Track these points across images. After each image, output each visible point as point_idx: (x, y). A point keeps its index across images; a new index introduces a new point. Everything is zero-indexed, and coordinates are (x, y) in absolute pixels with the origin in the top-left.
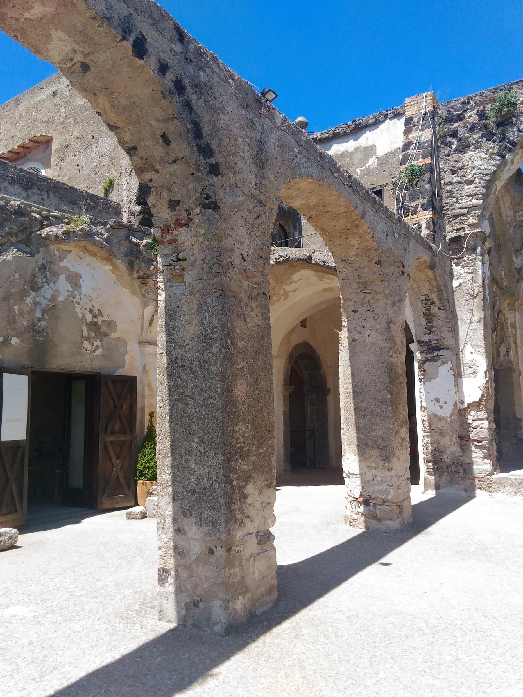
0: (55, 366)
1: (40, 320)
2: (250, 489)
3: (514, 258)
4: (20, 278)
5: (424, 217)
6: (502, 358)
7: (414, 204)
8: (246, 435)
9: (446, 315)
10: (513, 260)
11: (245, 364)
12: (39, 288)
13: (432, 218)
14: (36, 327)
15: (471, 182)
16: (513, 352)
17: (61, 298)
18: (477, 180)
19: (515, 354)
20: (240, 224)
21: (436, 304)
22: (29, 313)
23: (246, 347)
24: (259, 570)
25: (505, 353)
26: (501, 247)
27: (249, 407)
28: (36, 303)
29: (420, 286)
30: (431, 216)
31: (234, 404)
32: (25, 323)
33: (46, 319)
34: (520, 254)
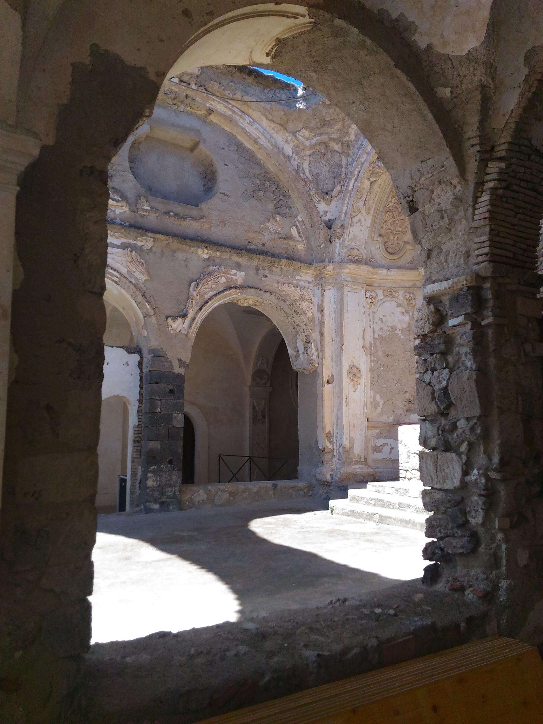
3: (322, 207)
6: (301, 356)
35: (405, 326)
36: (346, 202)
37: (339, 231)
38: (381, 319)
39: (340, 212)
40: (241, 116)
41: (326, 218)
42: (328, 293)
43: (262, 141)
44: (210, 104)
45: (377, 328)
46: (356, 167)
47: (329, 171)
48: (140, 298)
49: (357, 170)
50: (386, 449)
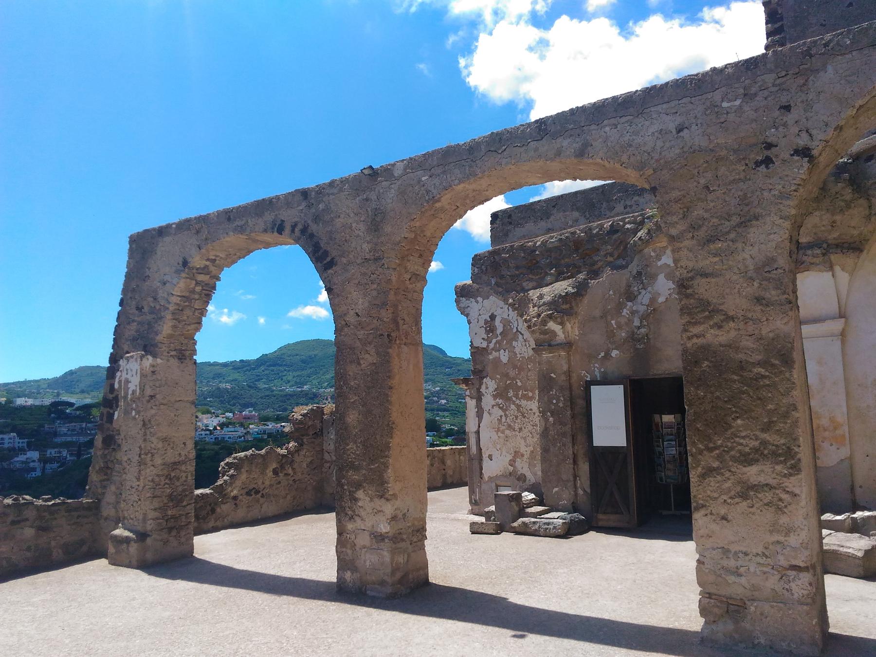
0: (660, 372)
1: (639, 328)
2: (360, 494)
4: (614, 294)
8: (358, 452)
11: (357, 398)
12: (636, 297)
14: (636, 336)
17: (661, 299)
20: (352, 291)
22: (627, 324)
23: (358, 385)
24: (370, 561)
27: (360, 431)
28: (633, 313)
31: (346, 429)
32: (623, 334)
33: (645, 325)
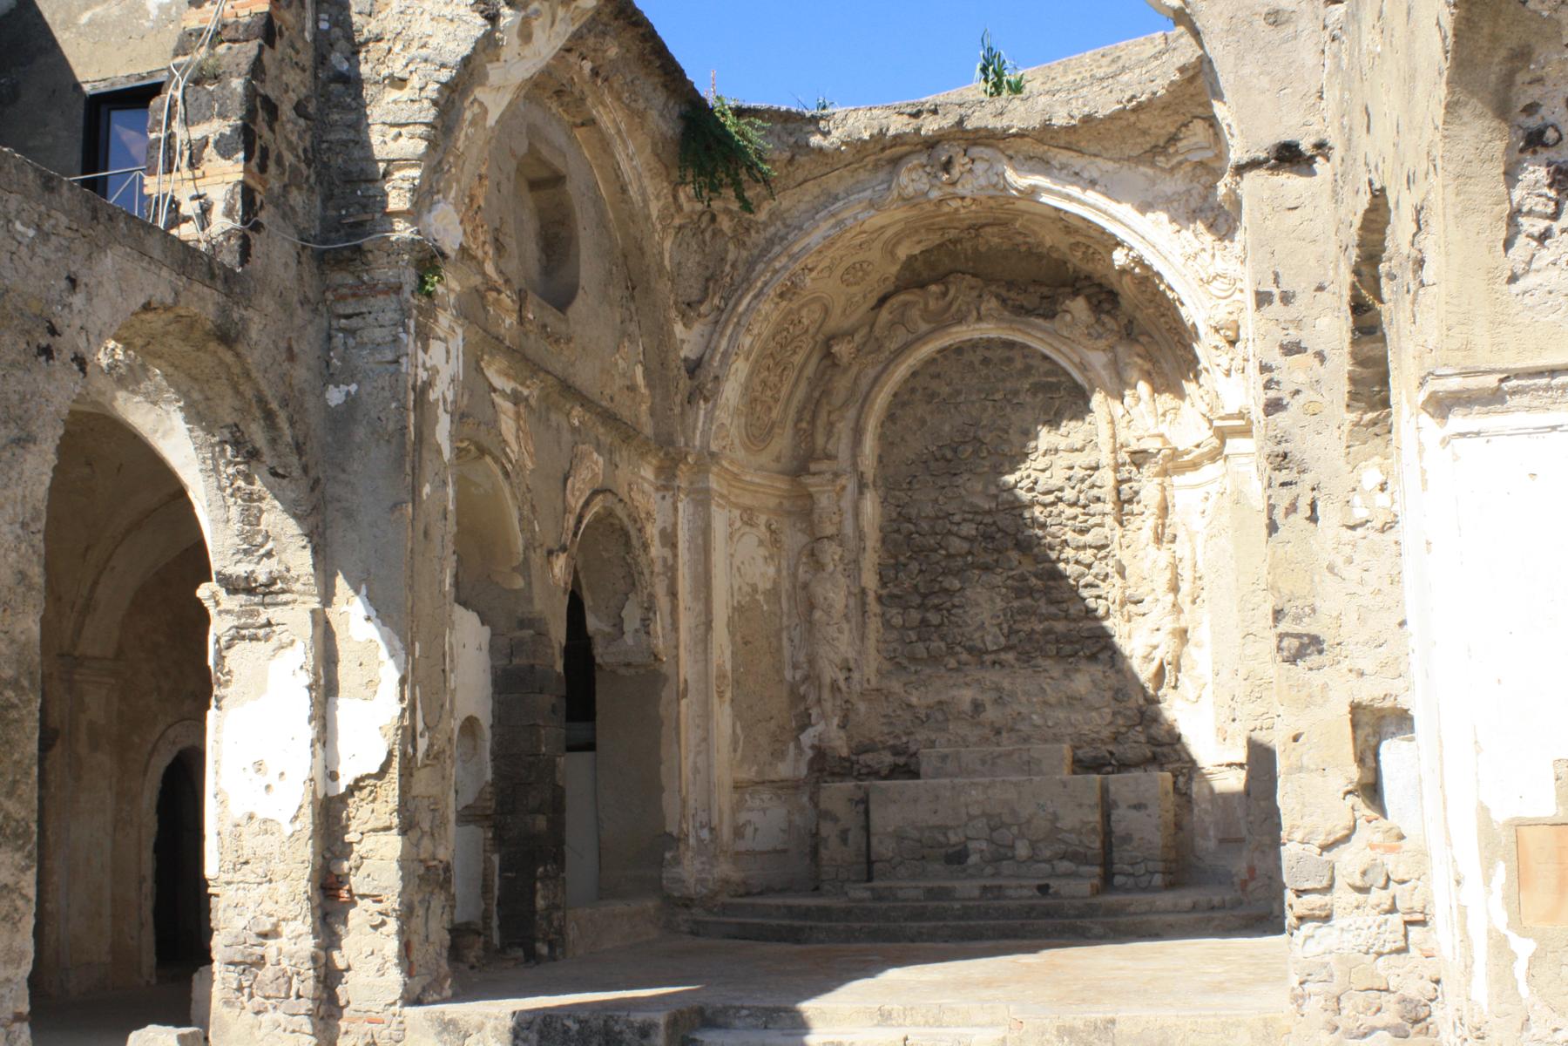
3: (679, 328)
5: (219, 179)
6: (629, 639)
7: (197, 132)
9: (293, 496)
10: (671, 333)
13: (240, 182)
15: (400, 83)
16: (662, 620)
18: (415, 81)
19: (669, 627)
21: (264, 458)
25: (637, 624)
26: (633, 289)
29: (210, 394)
30: (240, 177)
34: (699, 315)
35: (769, 586)
36: (728, 332)
37: (709, 386)
38: (739, 569)
39: (715, 349)
40: (624, 142)
41: (682, 355)
42: (680, 505)
43: (633, 191)
44: (598, 112)
45: (736, 587)
46: (762, 273)
47: (699, 263)
48: (527, 511)
49: (763, 279)
50: (749, 831)
